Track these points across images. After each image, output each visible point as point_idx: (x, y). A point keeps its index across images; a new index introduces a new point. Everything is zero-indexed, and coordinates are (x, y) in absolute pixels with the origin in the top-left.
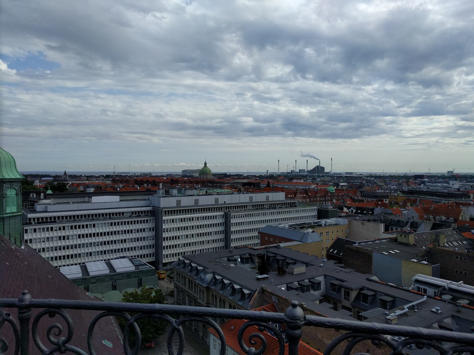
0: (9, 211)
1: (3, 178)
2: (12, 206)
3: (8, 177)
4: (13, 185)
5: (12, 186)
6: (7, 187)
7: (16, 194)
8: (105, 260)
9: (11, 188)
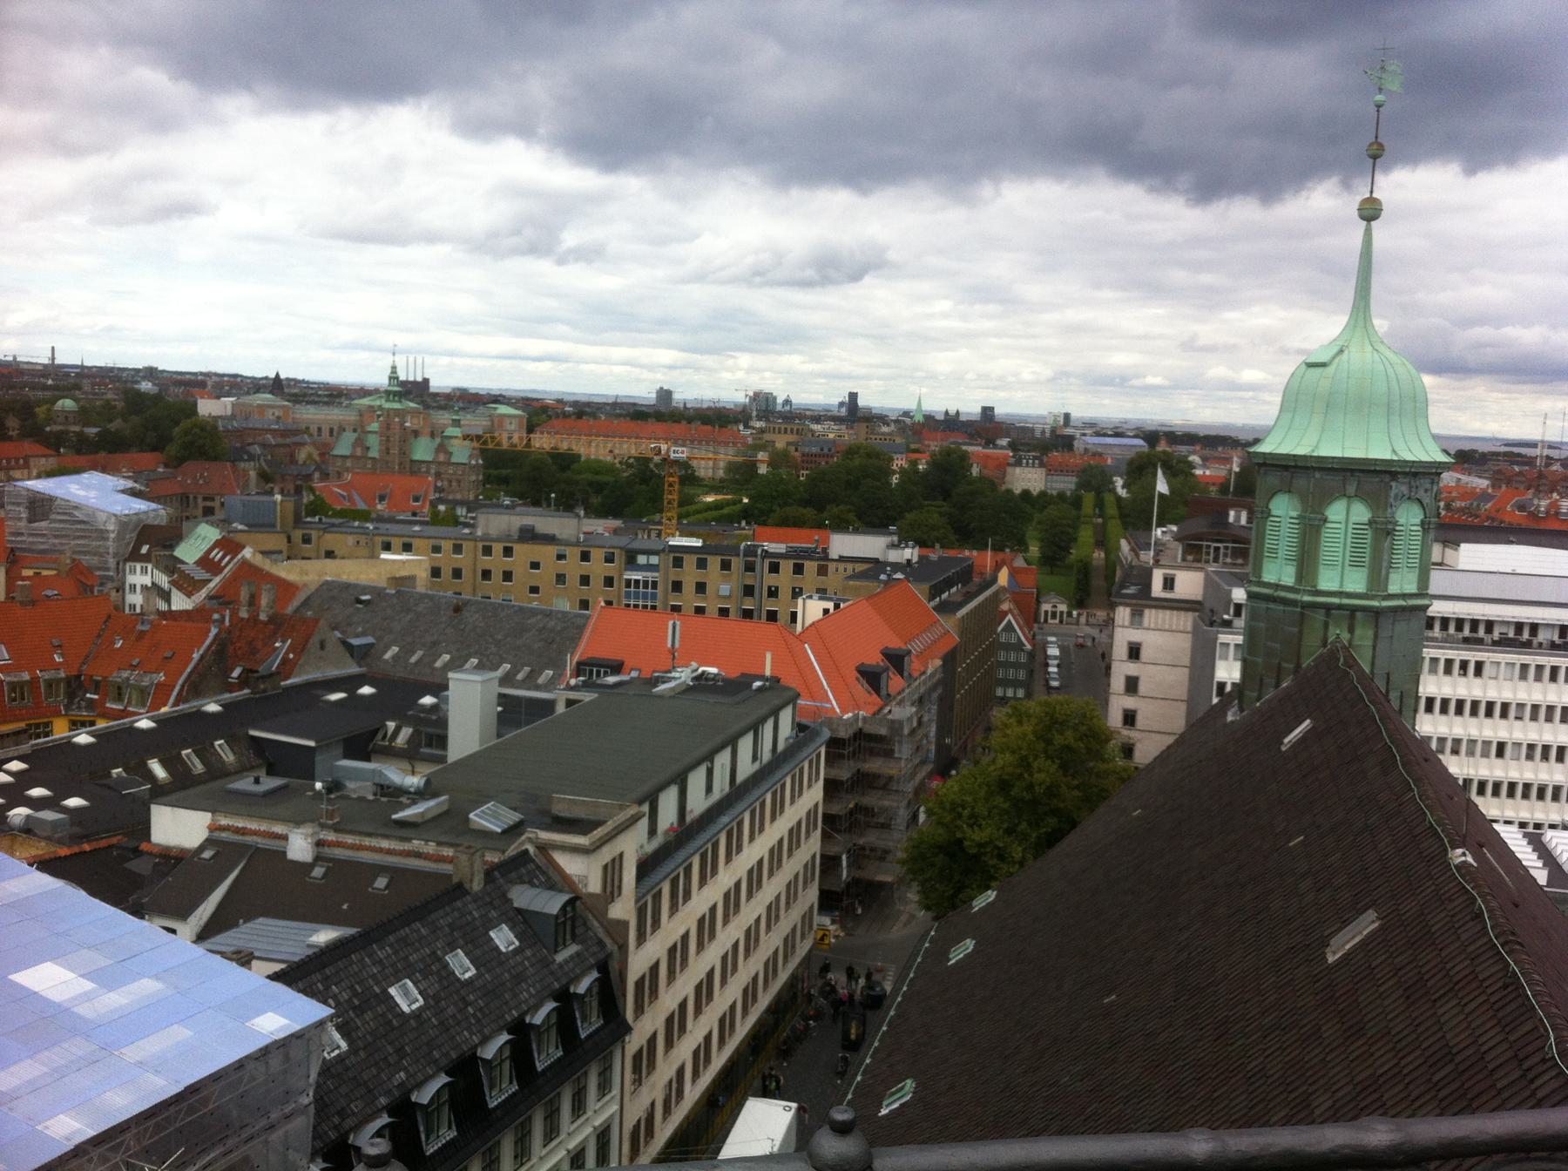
0: (1395, 587)
1: (1395, 458)
2: (1406, 569)
3: (1409, 457)
4: (1417, 487)
5: (1414, 489)
6: (1400, 494)
7: (1423, 523)
8: (1523, 825)
9: (1409, 498)
